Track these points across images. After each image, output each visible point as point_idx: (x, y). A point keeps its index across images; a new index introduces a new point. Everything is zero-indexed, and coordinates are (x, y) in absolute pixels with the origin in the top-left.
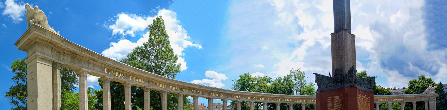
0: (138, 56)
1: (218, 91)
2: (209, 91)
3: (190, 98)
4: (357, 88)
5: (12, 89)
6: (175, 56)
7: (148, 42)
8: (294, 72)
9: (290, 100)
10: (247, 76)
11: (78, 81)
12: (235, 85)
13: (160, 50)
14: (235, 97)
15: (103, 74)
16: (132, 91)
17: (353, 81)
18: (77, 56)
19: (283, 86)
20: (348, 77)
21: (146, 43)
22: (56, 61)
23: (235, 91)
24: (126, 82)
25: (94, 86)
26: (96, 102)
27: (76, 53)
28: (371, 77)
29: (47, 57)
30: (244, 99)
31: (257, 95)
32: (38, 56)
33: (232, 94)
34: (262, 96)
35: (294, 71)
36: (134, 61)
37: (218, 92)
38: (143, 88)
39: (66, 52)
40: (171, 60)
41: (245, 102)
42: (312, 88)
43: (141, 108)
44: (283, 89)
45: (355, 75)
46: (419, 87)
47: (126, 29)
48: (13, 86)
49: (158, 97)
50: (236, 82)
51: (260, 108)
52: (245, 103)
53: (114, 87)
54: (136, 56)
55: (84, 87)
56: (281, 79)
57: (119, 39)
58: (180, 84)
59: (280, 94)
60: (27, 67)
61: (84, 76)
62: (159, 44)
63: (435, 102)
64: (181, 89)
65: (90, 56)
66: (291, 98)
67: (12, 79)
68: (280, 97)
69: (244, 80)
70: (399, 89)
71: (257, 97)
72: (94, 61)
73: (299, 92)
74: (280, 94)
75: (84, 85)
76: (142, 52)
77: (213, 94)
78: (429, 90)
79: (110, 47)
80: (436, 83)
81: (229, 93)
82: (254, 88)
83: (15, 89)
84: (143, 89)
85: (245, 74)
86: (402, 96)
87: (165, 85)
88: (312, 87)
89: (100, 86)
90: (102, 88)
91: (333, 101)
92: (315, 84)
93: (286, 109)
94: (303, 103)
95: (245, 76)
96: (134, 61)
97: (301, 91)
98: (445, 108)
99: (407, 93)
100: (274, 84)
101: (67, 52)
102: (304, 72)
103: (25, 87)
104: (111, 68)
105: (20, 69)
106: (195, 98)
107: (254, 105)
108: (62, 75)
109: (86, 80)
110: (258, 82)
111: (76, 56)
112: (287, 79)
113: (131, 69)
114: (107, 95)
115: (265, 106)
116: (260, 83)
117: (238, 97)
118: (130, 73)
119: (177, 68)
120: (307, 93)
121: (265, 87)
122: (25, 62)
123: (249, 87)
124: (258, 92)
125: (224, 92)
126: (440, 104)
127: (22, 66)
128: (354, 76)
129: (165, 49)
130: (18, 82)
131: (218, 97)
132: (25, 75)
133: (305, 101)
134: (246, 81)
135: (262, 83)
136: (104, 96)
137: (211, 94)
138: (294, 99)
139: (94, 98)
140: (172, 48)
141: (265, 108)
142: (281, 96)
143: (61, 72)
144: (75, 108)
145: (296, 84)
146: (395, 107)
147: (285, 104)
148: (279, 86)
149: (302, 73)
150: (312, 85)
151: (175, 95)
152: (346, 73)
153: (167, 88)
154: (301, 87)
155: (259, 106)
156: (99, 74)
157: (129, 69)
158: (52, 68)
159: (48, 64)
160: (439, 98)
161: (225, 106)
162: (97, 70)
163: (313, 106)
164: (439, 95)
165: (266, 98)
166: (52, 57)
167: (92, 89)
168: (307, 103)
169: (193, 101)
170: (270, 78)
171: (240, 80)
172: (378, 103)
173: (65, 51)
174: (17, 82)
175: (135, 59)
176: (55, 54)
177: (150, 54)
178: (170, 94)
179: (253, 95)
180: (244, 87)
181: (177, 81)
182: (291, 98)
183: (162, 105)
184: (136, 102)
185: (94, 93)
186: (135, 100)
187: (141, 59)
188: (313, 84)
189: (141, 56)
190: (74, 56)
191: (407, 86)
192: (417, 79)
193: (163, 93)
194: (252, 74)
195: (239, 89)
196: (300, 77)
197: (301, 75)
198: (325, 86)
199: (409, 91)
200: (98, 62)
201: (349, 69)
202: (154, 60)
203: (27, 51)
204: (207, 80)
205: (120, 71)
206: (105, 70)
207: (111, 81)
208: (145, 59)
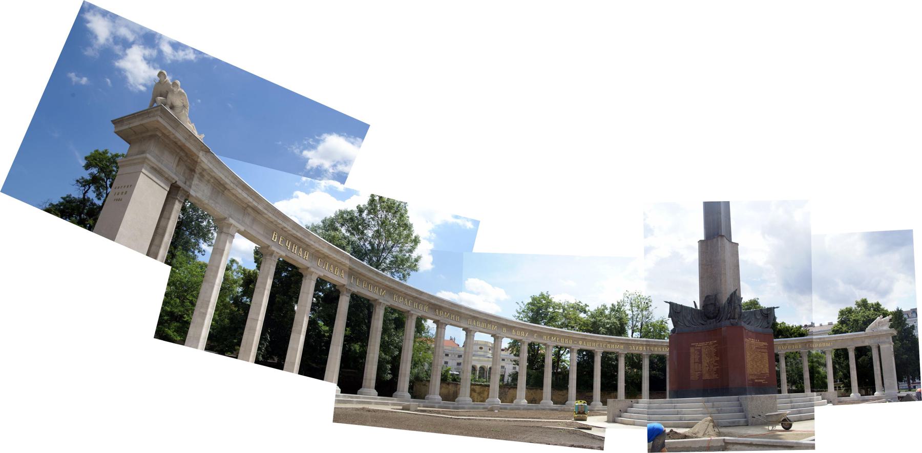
0: (342, 225)
2: (470, 315)
3: (430, 324)
4: (743, 327)
5: (67, 202)
6: (416, 237)
7: (367, 206)
11: (213, 239)
13: (387, 222)
15: (268, 242)
16: (317, 288)
17: (737, 316)
18: (225, 192)
19: (608, 321)
20: (726, 309)
21: (362, 206)
22: (180, 183)
24: (308, 268)
25: (243, 260)
26: (238, 292)
27: (226, 186)
28: (768, 308)
29: (165, 170)
30: (535, 339)
32: (149, 162)
34: (569, 337)
36: (333, 233)
37: (487, 320)
38: (340, 286)
39: (206, 176)
40: (406, 243)
41: (537, 345)
43: (327, 326)
44: (608, 326)
45: (740, 306)
46: (858, 320)
47: (338, 162)
48: (73, 196)
49: (366, 312)
51: (563, 357)
53: (281, 272)
54: (338, 225)
55: (222, 255)
56: (607, 309)
57: (313, 188)
58: (414, 294)
59: (603, 334)
60: (117, 171)
61: (228, 234)
62: (387, 211)
63: (892, 346)
64: (416, 304)
65: (251, 200)
67: (78, 181)
68: (602, 340)
70: (821, 325)
71: (560, 337)
72: (258, 212)
74: (602, 334)
75: (224, 250)
76: (352, 220)
78: (877, 324)
79: (292, 198)
80: (890, 310)
81: (508, 324)
83: (74, 204)
84: (340, 290)
86: (827, 337)
87: (385, 291)
89: (255, 262)
90: (258, 267)
93: (613, 363)
94: (644, 353)
96: (333, 233)
98: (912, 355)
99: (836, 332)
100: (592, 316)
101: (207, 177)
103: (95, 209)
104: (286, 235)
105: (102, 170)
106: (440, 325)
108: (183, 214)
109: (231, 242)
111: (223, 190)
112: (616, 308)
113: (325, 247)
114: (265, 284)
117: (525, 334)
118: (320, 253)
119: (413, 263)
121: (576, 321)
122: (118, 161)
123: (546, 317)
124: (562, 328)
125: (498, 321)
126: (901, 349)
127: (108, 166)
128: (738, 307)
129: (396, 223)
130: (86, 192)
131: (485, 330)
132: (107, 185)
136: (257, 285)
137: (473, 322)
138: (627, 344)
139: (235, 282)
140: (411, 223)
143: (184, 209)
144: (190, 291)
145: (632, 317)
146: (816, 359)
147: (611, 353)
148: (601, 320)
149: (644, 298)
150: (662, 321)
151: (401, 313)
152: (724, 302)
153: (387, 297)
154: (642, 323)
155: (563, 354)
156: (259, 240)
157: (320, 245)
158: (167, 195)
159: (163, 185)
160: (899, 337)
161: (498, 349)
162: (256, 231)
164: (899, 332)
165: (575, 340)
166: (175, 174)
167: (237, 263)
168: (654, 353)
169: (435, 331)
172: (783, 352)
173: (204, 173)
174: (84, 192)
175: (336, 229)
176: (183, 171)
177: (367, 226)
178: (392, 309)
179: (553, 333)
180: (537, 316)
181: (410, 288)
183: (371, 329)
184: (319, 312)
185: (240, 273)
186: (319, 308)
187: (346, 231)
189: (348, 227)
190: (221, 190)
191: (835, 320)
192: (854, 306)
193: (377, 306)
196: (640, 306)
197: (643, 303)
198: (687, 324)
199: (841, 328)
200: (264, 217)
201: (728, 296)
202: (372, 238)
203: (130, 144)
205: (301, 244)
206: (274, 235)
207: (279, 259)
208: (355, 233)
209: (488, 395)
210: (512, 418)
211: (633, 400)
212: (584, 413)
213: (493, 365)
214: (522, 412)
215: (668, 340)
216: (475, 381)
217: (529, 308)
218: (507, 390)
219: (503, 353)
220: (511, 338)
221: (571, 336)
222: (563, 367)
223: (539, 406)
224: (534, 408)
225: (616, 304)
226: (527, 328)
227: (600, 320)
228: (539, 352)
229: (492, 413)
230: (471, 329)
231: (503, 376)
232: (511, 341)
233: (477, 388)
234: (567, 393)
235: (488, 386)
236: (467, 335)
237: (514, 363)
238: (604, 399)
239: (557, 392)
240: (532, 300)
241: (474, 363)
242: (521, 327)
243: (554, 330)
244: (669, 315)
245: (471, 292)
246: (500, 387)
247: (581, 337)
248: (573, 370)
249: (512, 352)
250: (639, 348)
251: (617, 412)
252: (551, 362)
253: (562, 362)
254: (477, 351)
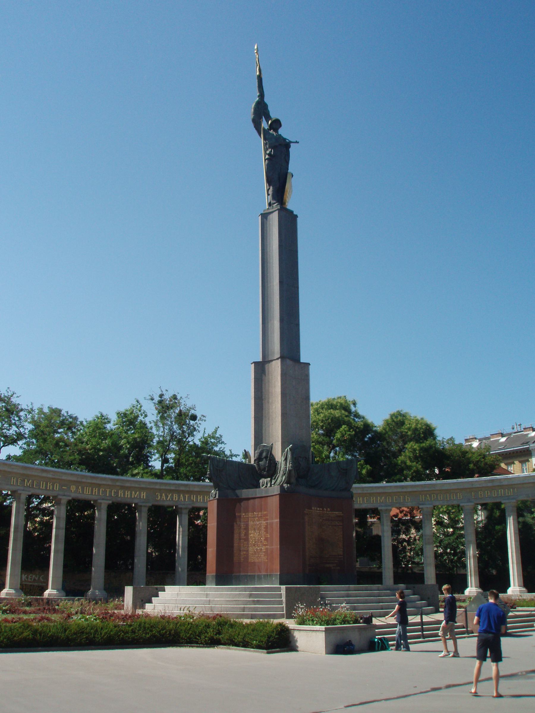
9: (140, 494)
34: (53, 478)
172: (428, 506)
247: (75, 479)
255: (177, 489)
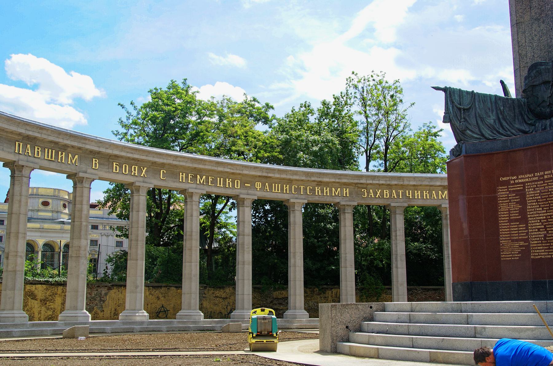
1: (57, 140)
2: (20, 134)
8: (360, 86)
9: (342, 191)
10: (178, 93)
12: (131, 121)
14: (125, 168)
19: (316, 137)
23: (130, 145)
31: (213, 168)
33: (117, 156)
34: (233, 173)
35: (359, 82)
37: (56, 143)
41: (166, 193)
42: (432, 146)
44: (315, 148)
50: (134, 113)
51: (222, 218)
52: (165, 197)
56: (311, 112)
59: (305, 165)
66: (346, 185)
68: (304, 178)
69: (166, 108)
73: (381, 162)
77: (33, 149)
81: (103, 150)
82: (203, 138)
85: (173, 86)
88: (432, 140)
91: (522, 195)
92: (441, 130)
93: (329, 226)
94: (393, 204)
95: (173, 94)
97: (385, 156)
100: (282, 129)
102: (401, 84)
107: (201, 206)
110: (222, 117)
112: (332, 110)
115: (244, 212)
116: (230, 122)
117: (140, 171)
120: (411, 165)
121: (247, 141)
123: (184, 133)
124: (218, 156)
125: (80, 145)
131: (53, 165)
133: (404, 194)
134: (174, 112)
135: (235, 123)
137: (25, 147)
141: (244, 217)
142: (307, 174)
145: (367, 129)
147: (323, 206)
148: (300, 136)
149: (390, 87)
150: (429, 134)
154: (387, 139)
163: (435, 215)
168: (412, 203)
170: (268, 107)
171: (152, 106)
179: (201, 166)
180: (165, 132)
182: (346, 185)
188: (434, 131)
194: (200, 88)
195: (147, 142)
196: (383, 104)
197: (388, 97)
198: (487, 133)
204: (13, 88)
209: (63, 304)
210: (116, 350)
211: (374, 305)
212: (269, 335)
213: (72, 238)
214: (137, 337)
215: (445, 175)
216: (34, 275)
217: (146, 114)
218: (104, 291)
219: (93, 212)
220: (111, 181)
221: (238, 172)
222: (224, 238)
223: (175, 323)
224: (164, 327)
225: (331, 100)
226: (144, 158)
227: (297, 138)
228: (171, 208)
229: (73, 341)
230: (21, 163)
231: (94, 262)
232: (111, 187)
233: (39, 290)
234: (234, 293)
235: (64, 284)
236: (13, 177)
237: (119, 233)
238: (311, 304)
239: (210, 292)
240: (153, 98)
241: (30, 236)
242: (129, 155)
243: (202, 160)
244: (444, 117)
245: (21, 84)
246: (90, 285)
248: (243, 244)
249: (114, 210)
250: (382, 194)
251: (341, 330)
252: (196, 229)
253: (220, 228)
254: (38, 211)
255: (388, 183)
